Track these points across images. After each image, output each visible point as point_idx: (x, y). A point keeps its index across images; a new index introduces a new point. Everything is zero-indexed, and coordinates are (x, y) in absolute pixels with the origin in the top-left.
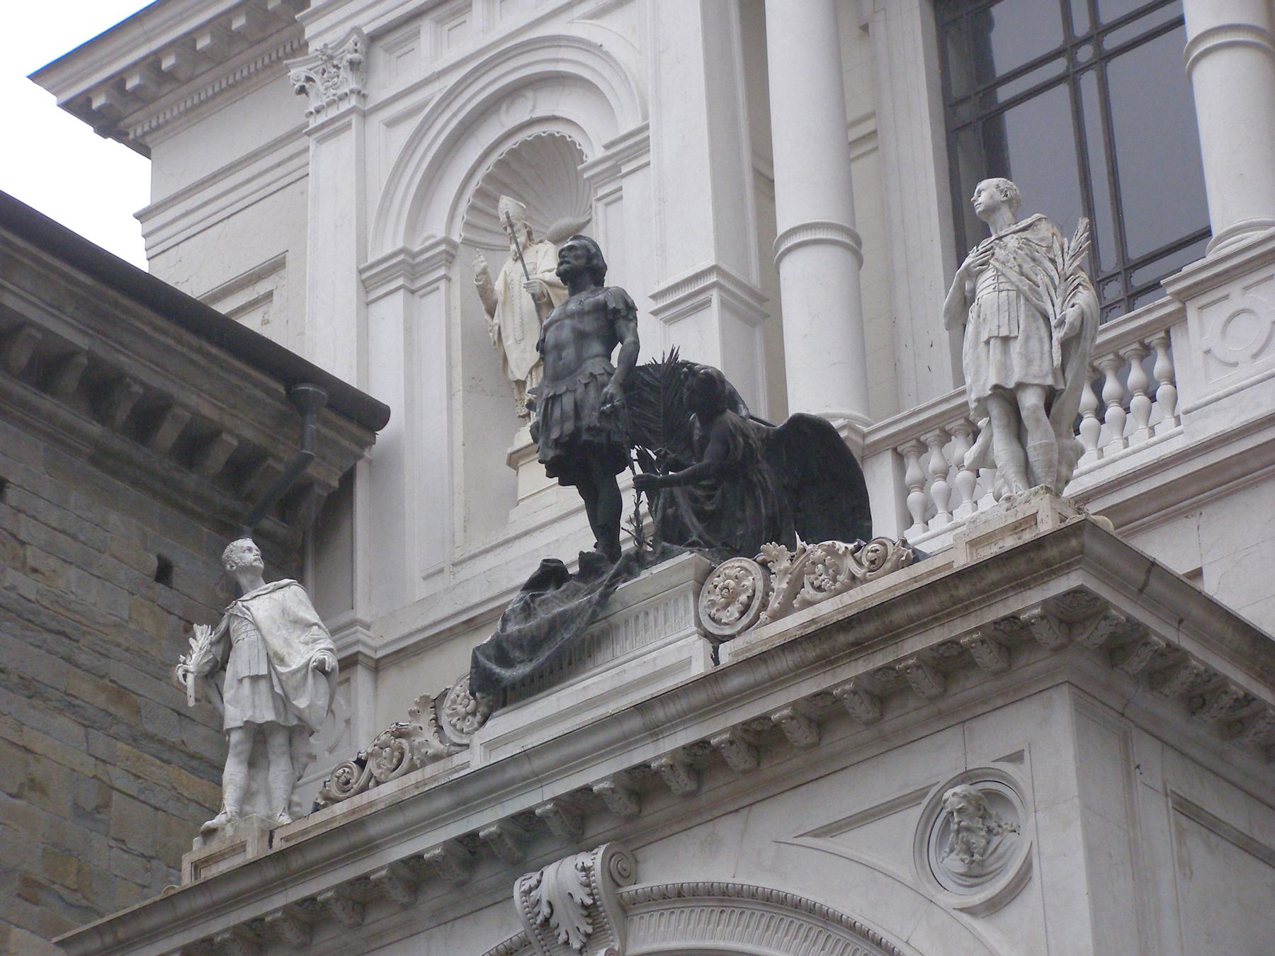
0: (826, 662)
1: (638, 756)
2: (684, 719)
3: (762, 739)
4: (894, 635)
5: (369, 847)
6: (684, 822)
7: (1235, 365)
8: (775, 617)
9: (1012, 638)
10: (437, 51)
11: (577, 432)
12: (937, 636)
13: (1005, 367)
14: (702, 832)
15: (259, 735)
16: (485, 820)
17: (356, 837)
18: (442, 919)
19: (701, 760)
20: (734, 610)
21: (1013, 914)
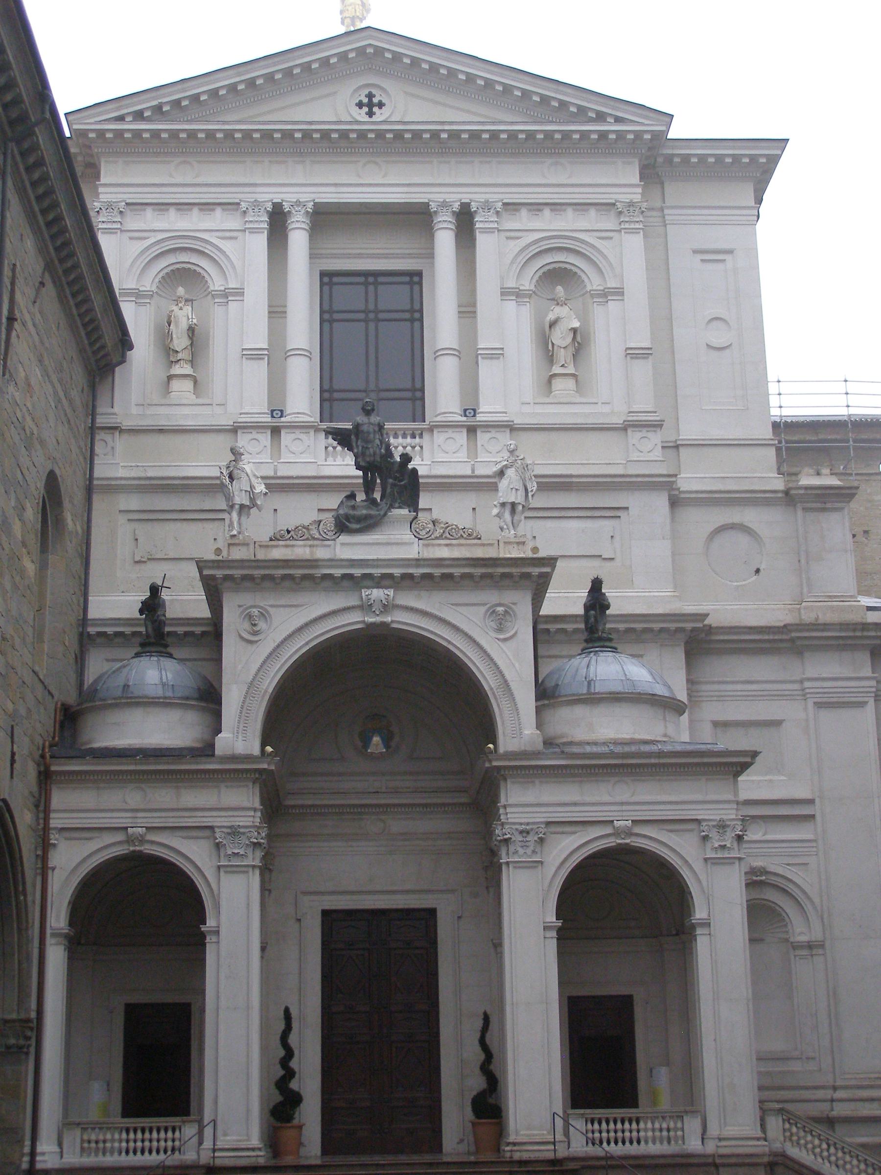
0: (474, 566)
1: (410, 571)
2: (429, 566)
4: (496, 566)
5: (317, 567)
6: (411, 588)
7: (22, 235)
8: (437, 538)
9: (526, 576)
10: (150, 220)
11: (374, 461)
12: (507, 570)
13: (516, 498)
14: (416, 593)
15: (242, 506)
16: (357, 572)
17: (314, 563)
18: (325, 590)
19: (428, 577)
20: (423, 533)
21: (509, 643)
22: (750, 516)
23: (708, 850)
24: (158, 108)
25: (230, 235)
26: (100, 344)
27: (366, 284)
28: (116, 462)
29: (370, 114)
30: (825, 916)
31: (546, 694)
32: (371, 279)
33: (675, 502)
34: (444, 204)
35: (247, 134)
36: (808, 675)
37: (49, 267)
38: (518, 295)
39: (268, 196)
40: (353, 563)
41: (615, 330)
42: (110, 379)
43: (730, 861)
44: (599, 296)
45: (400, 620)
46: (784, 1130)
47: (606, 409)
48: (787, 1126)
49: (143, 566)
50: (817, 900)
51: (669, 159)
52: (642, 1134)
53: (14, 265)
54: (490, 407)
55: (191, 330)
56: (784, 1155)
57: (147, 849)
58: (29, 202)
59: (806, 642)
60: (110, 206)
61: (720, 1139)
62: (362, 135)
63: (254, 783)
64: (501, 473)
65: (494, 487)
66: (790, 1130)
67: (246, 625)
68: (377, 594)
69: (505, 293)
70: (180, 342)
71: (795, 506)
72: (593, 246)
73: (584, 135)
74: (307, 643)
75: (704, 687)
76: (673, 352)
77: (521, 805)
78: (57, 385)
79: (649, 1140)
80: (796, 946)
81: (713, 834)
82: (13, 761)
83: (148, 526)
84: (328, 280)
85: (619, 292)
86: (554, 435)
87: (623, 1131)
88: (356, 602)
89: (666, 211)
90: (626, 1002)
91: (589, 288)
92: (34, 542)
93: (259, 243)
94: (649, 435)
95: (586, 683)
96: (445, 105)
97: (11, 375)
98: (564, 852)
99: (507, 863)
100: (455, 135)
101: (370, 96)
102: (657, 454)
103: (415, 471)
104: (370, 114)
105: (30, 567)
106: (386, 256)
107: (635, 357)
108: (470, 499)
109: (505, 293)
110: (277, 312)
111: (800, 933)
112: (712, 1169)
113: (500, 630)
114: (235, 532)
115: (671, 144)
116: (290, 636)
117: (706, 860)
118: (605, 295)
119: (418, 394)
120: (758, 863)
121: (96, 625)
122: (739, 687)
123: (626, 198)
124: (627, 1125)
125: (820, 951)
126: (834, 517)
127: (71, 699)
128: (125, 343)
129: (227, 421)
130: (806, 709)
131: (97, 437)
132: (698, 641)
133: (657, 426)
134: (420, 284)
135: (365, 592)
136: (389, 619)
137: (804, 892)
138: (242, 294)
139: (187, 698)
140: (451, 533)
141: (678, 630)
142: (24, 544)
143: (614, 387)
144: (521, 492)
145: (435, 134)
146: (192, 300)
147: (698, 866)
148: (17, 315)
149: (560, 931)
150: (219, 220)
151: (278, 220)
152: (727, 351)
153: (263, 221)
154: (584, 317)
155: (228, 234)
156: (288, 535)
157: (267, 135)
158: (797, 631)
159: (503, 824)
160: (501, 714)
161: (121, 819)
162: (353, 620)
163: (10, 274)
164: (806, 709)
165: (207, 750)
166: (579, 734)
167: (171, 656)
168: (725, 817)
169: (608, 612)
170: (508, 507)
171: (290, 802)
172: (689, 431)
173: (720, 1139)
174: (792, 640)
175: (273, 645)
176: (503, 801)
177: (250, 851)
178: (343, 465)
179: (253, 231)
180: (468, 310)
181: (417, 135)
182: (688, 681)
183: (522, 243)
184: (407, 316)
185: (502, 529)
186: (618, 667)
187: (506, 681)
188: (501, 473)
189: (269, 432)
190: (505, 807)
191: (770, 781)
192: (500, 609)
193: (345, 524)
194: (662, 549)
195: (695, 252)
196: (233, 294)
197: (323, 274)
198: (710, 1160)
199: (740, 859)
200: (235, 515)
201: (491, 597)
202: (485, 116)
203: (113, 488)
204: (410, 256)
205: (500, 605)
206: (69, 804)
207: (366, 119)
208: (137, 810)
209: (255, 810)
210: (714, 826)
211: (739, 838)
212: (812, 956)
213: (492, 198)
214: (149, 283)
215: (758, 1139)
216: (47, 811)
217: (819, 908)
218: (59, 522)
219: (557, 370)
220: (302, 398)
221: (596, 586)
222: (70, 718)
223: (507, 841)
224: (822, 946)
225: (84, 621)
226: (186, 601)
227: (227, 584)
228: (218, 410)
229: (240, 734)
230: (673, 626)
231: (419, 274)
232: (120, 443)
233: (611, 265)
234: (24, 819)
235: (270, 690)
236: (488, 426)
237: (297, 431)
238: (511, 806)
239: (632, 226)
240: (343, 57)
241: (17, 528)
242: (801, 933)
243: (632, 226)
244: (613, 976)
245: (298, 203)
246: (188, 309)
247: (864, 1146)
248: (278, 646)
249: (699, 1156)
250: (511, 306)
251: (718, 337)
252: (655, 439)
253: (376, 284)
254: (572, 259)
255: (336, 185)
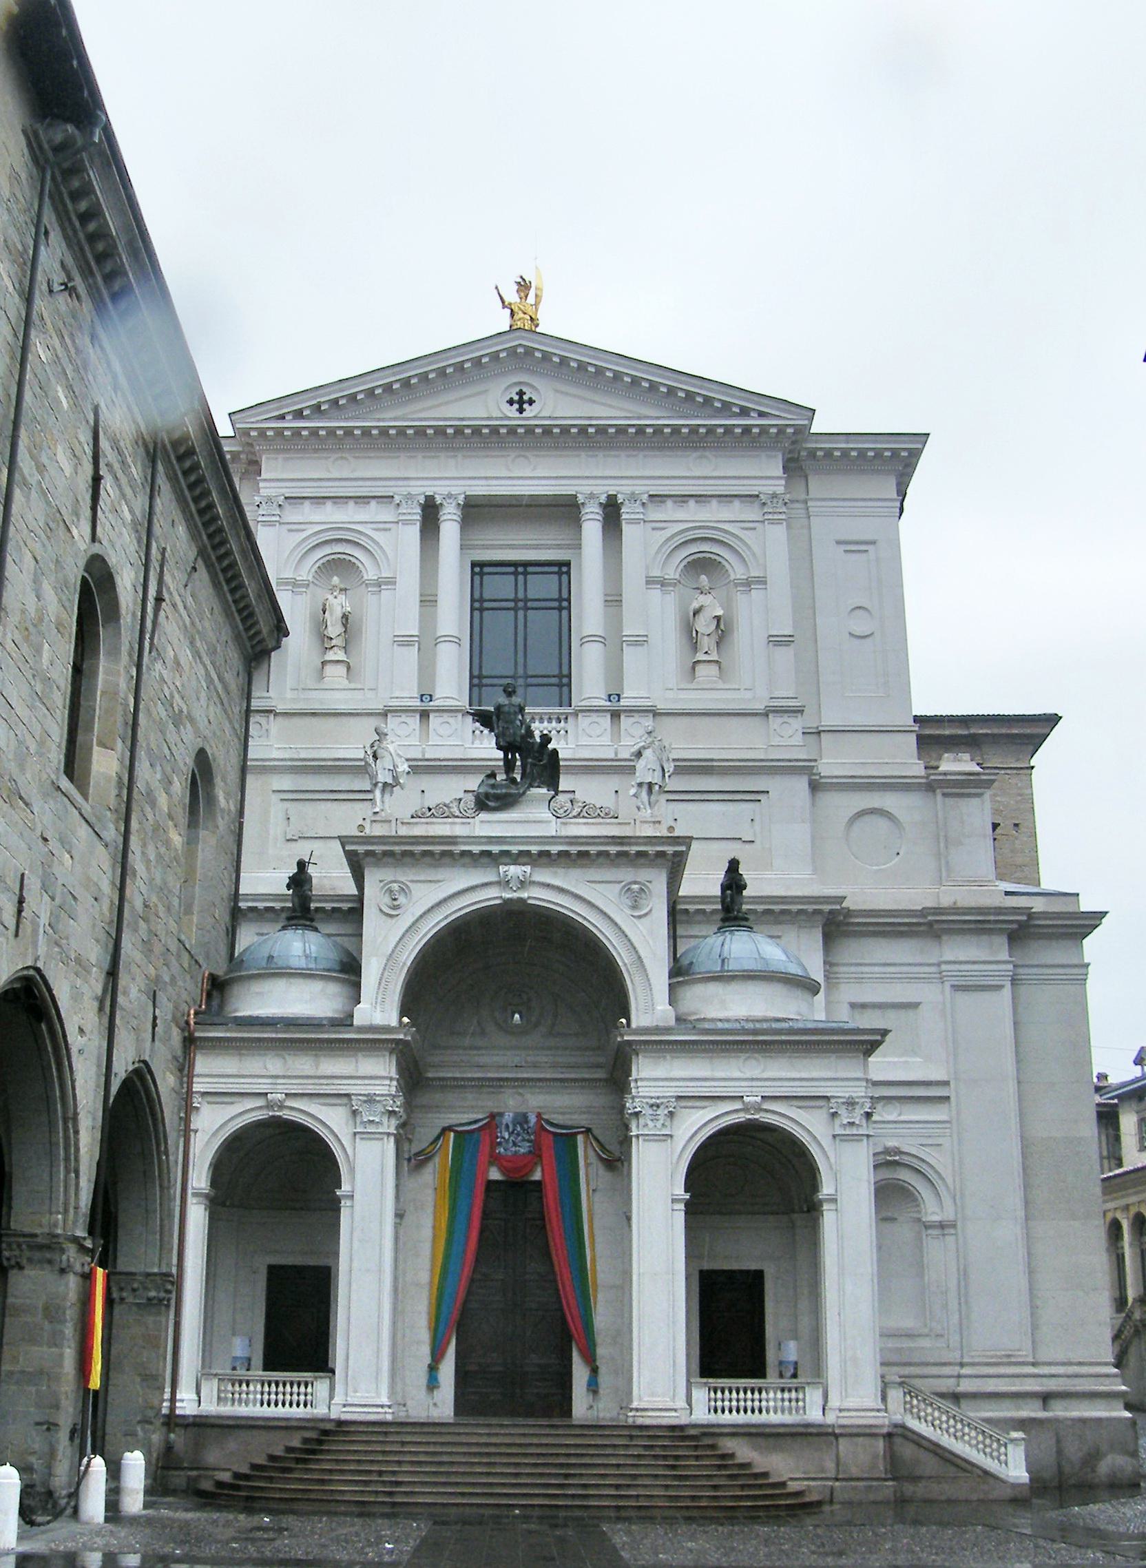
1: (547, 848)
3: (583, 855)
4: (630, 844)
5: (455, 844)
10: (307, 513)
15: (385, 784)
16: (495, 849)
18: (464, 866)
20: (561, 811)
22: (889, 801)
23: (837, 1127)
24: (317, 408)
25: (383, 527)
26: (254, 630)
27: (516, 574)
28: (268, 743)
29: (521, 410)
30: (958, 1197)
31: (680, 972)
32: (520, 569)
33: (815, 787)
34: (592, 496)
35: (401, 431)
36: (945, 958)
37: (202, 553)
38: (663, 583)
39: (420, 490)
40: (491, 840)
41: (756, 617)
42: (266, 666)
43: (857, 1138)
44: (742, 585)
45: (536, 896)
46: (905, 1403)
47: (748, 695)
48: (908, 1398)
49: (293, 844)
50: (949, 1181)
51: (812, 454)
52: (764, 1403)
53: (164, 549)
54: (632, 695)
55: (345, 617)
56: (903, 1426)
57: (286, 1114)
58: (182, 491)
59: (945, 926)
60: (269, 500)
61: (841, 1410)
62: (512, 430)
63: (391, 1053)
64: (639, 754)
65: (632, 770)
66: (911, 1403)
67: (387, 899)
68: (514, 871)
69: (650, 581)
70: (334, 629)
71: (934, 791)
72: (736, 537)
73: (728, 430)
74: (446, 918)
75: (842, 969)
76: (816, 641)
77: (651, 1078)
78: (210, 667)
79: (771, 1407)
80: (928, 1226)
81: (842, 1111)
82: (154, 1025)
83: (299, 805)
84: (479, 569)
85: (762, 581)
86: (695, 720)
87: (745, 1400)
88: (494, 878)
89: (810, 504)
90: (759, 1275)
91: (732, 577)
92: (182, 817)
93: (413, 533)
94: (790, 720)
95: (720, 961)
96: (594, 402)
97: (159, 654)
98: (695, 1126)
99: (637, 1136)
100: (602, 430)
101: (521, 393)
102: (798, 739)
103: (555, 752)
104: (521, 410)
105: (177, 839)
106: (536, 547)
107: (778, 644)
108: (614, 782)
109: (650, 581)
110: (428, 601)
111: (932, 1212)
112: (832, 1438)
113: (634, 907)
114: (377, 810)
115: (814, 438)
116: (429, 911)
117: (834, 1136)
118: (748, 584)
119: (565, 680)
120: (891, 1143)
121: (247, 901)
122: (877, 969)
123: (770, 490)
124: (749, 1395)
125: (952, 1231)
126: (975, 802)
127: (220, 972)
128: (281, 630)
129: (379, 706)
130: (943, 992)
131: (252, 720)
132: (836, 924)
133: (799, 711)
134: (568, 573)
135: (502, 869)
136: (525, 895)
137: (937, 1172)
138: (395, 583)
139: (328, 970)
140: (587, 812)
141: (816, 912)
142: (171, 817)
143: (755, 675)
144: (659, 773)
145: (583, 430)
146: (346, 590)
147: (826, 1142)
148: (166, 595)
149: (688, 1204)
150: (374, 512)
151: (430, 512)
152: (868, 640)
153: (416, 514)
154: (728, 604)
155: (381, 526)
156: (430, 813)
157: (420, 431)
158: (934, 914)
159: (633, 1098)
160: (634, 990)
161: (261, 1086)
162: (492, 896)
163: (159, 557)
164: (943, 992)
165: (345, 1021)
166: (712, 1012)
167: (316, 930)
168: (854, 1095)
169: (745, 893)
170: (645, 789)
171: (430, 1075)
172: (830, 719)
173: (841, 1410)
174: (930, 924)
175: (412, 920)
176: (634, 1075)
177: (385, 1120)
178: (486, 748)
179: (406, 523)
180: (614, 600)
181: (565, 430)
182: (825, 963)
183: (668, 533)
184: (556, 604)
185: (639, 808)
186: (751, 946)
187: (640, 957)
188: (639, 754)
189: (418, 717)
190: (636, 1080)
191: (906, 1062)
192: (635, 887)
193: (486, 802)
194: (799, 833)
195: (839, 543)
196: (387, 583)
197: (474, 565)
198: (830, 1430)
199: (868, 1136)
200: (378, 793)
201: (626, 874)
202: (630, 411)
203: (267, 769)
204: (559, 547)
205: (635, 883)
206: (211, 1070)
207: (517, 415)
208: (277, 1077)
209: (391, 1079)
210: (843, 1103)
211: (868, 1115)
212: (944, 1235)
213: (638, 490)
214: (306, 573)
215: (878, 1410)
216: (190, 1076)
217: (951, 1187)
218: (211, 800)
219: (700, 656)
220: (452, 686)
221: (733, 866)
222: (218, 987)
223: (637, 1114)
224: (954, 1226)
225: (236, 896)
226: (332, 877)
227: (368, 859)
228: (370, 694)
229: (379, 1007)
230: (810, 908)
231: (568, 564)
232: (275, 725)
233: (754, 554)
234: (166, 1082)
235: (409, 964)
236: (631, 711)
237: (445, 715)
238: (642, 1079)
239: (776, 517)
240: (495, 356)
241: (163, 800)
242: (933, 1213)
243: (776, 517)
244: (742, 1251)
245: (450, 496)
246: (342, 598)
247: (988, 1421)
248: (417, 920)
249: (820, 1426)
250: (655, 594)
251: (861, 625)
252: (796, 724)
253: (525, 574)
254: (716, 549)
255: (486, 478)
